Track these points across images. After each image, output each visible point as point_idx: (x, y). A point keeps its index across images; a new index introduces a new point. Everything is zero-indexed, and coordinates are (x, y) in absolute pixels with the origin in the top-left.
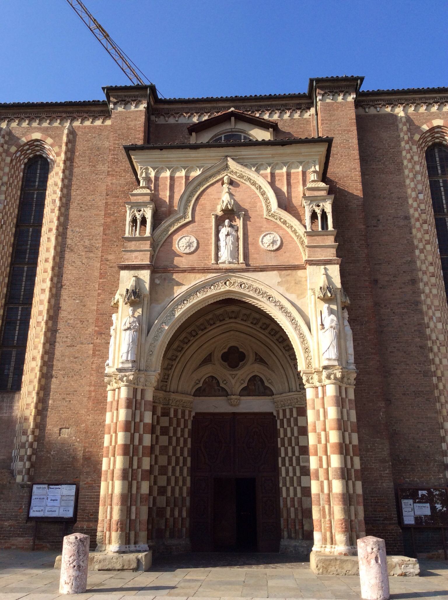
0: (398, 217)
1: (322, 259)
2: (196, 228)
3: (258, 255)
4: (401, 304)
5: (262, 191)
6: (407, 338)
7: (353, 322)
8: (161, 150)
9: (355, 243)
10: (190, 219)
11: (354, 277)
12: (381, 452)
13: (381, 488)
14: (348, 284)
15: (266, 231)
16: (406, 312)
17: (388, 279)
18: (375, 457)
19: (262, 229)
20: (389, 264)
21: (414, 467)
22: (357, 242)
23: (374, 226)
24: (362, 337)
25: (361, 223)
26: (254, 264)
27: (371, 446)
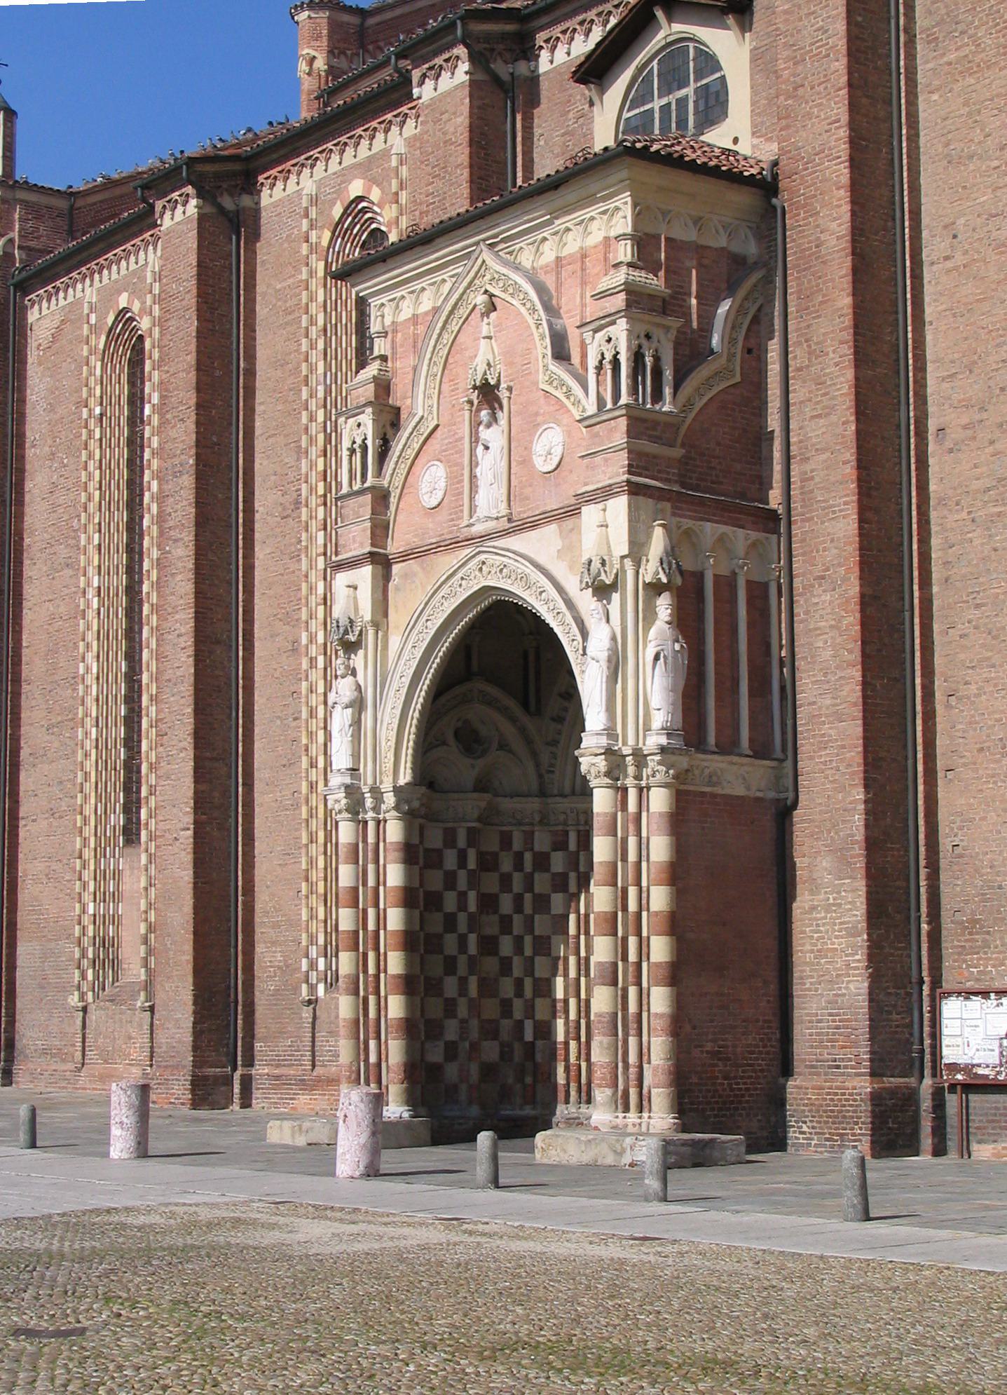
0: (997, 215)
1: (600, 485)
2: (446, 441)
3: (530, 489)
4: (989, 489)
5: (536, 317)
6: (997, 590)
7: (820, 585)
8: (384, 261)
9: (831, 355)
10: (435, 422)
11: (824, 457)
12: (851, 910)
13: (844, 995)
14: (812, 478)
15: (544, 423)
16: (999, 514)
17: (967, 421)
18: (841, 923)
19: (540, 419)
20: (971, 371)
21: (987, 937)
22: (834, 352)
23: (947, 258)
24: (833, 623)
25: (842, 290)
26: (524, 512)
27: (834, 899)
